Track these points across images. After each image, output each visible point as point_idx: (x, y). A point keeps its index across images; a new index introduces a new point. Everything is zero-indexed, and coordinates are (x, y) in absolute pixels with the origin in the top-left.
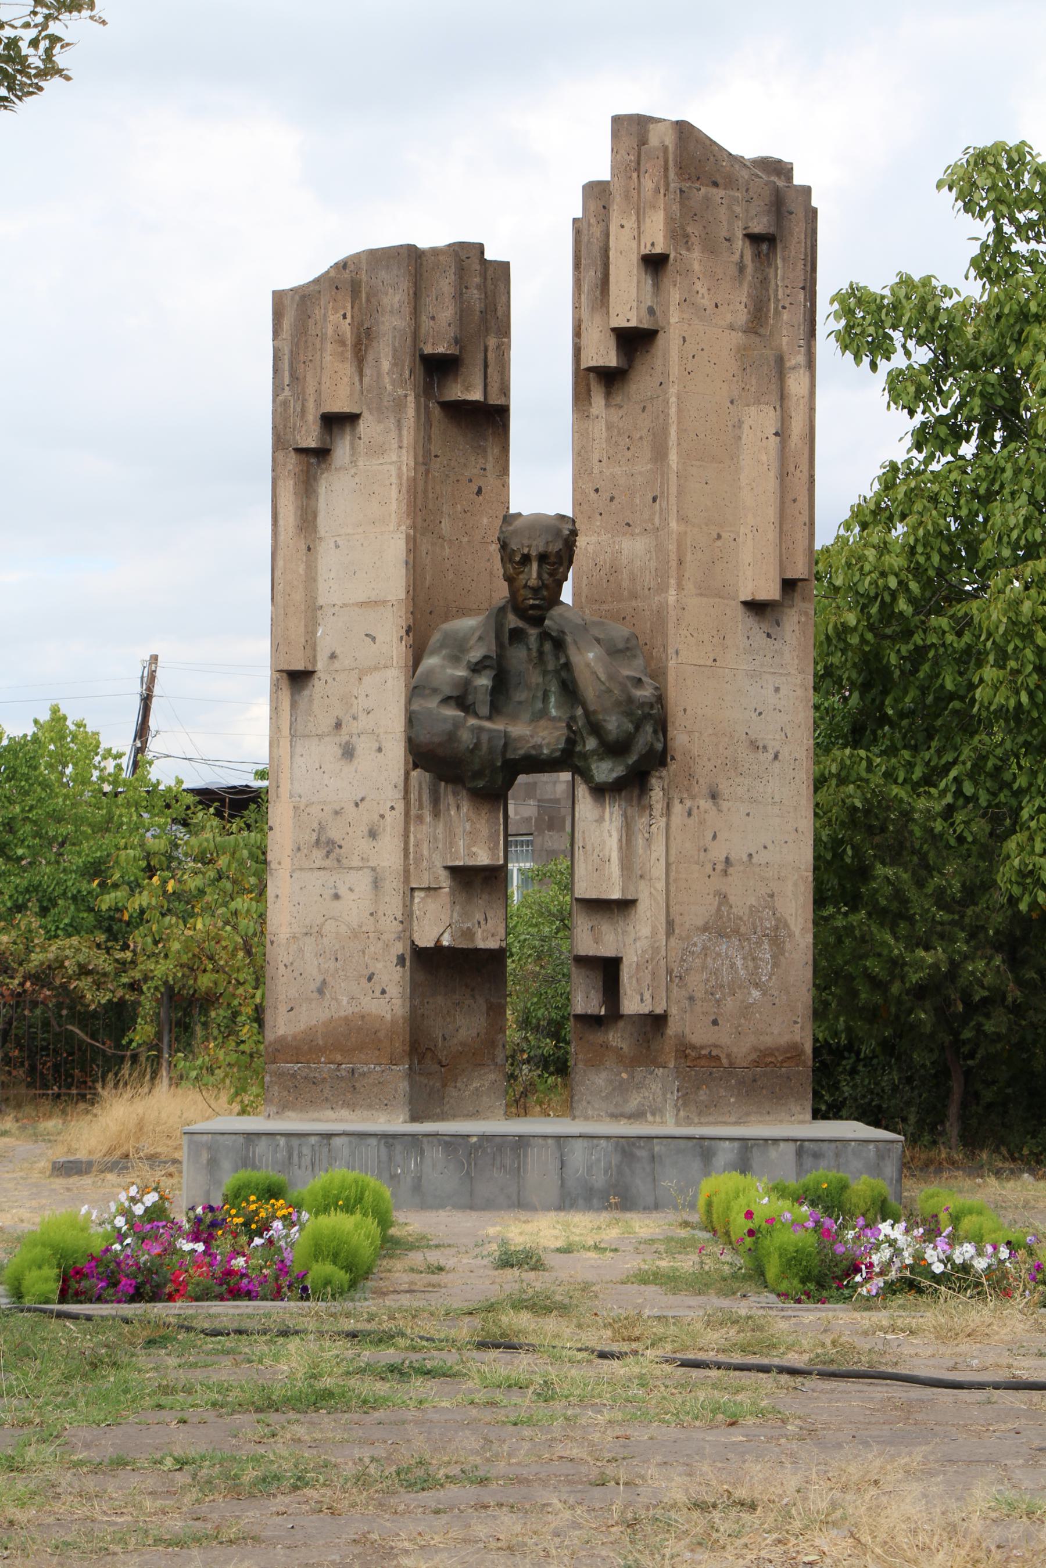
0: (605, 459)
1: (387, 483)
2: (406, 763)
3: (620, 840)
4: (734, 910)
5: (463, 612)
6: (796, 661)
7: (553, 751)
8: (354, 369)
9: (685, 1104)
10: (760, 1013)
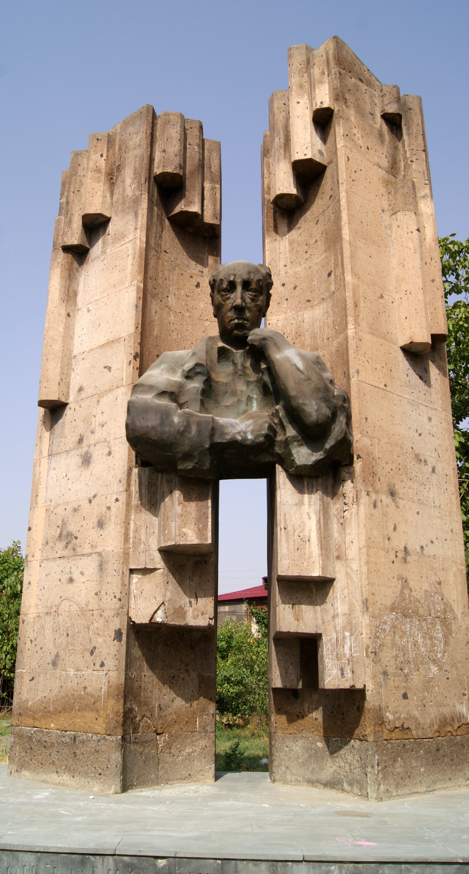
0: (289, 264)
1: (126, 256)
2: (130, 461)
3: (319, 522)
4: (414, 593)
7: (257, 436)
8: (106, 188)
9: (385, 778)
10: (439, 686)
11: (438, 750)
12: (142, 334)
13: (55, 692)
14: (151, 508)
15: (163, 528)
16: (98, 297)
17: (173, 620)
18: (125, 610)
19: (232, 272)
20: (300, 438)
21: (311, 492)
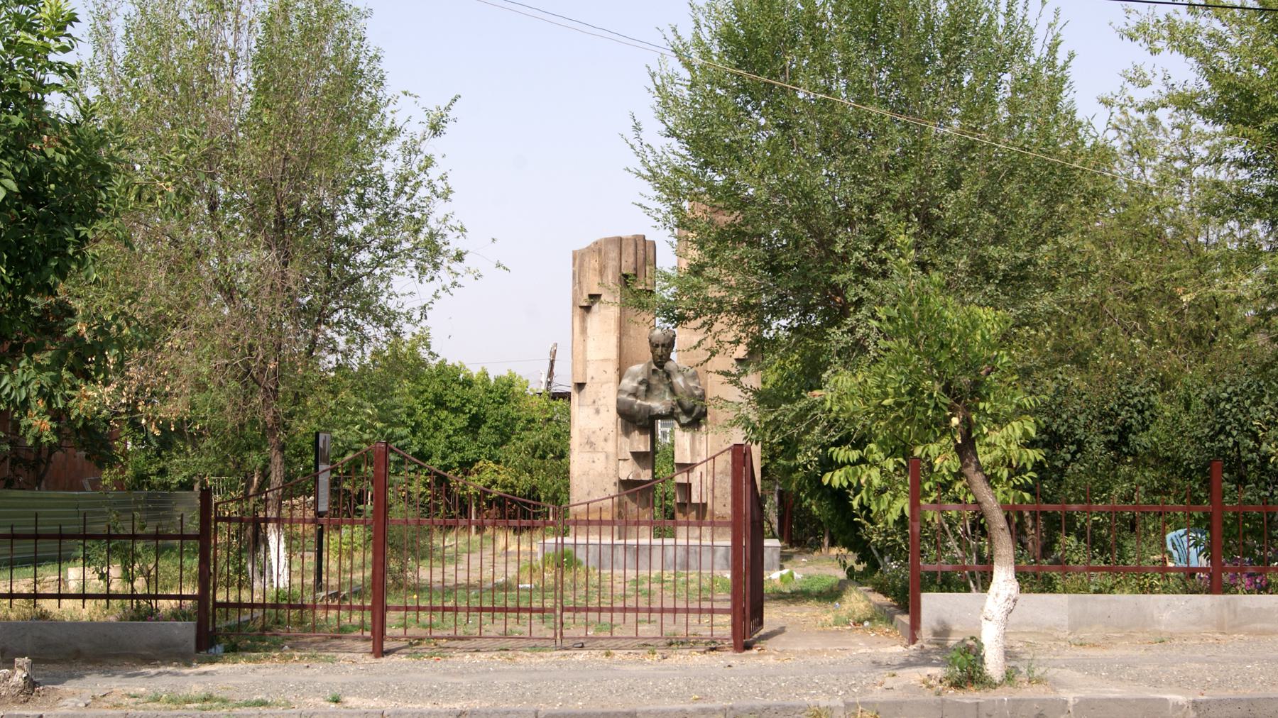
5: (638, 362)
15: (631, 444)
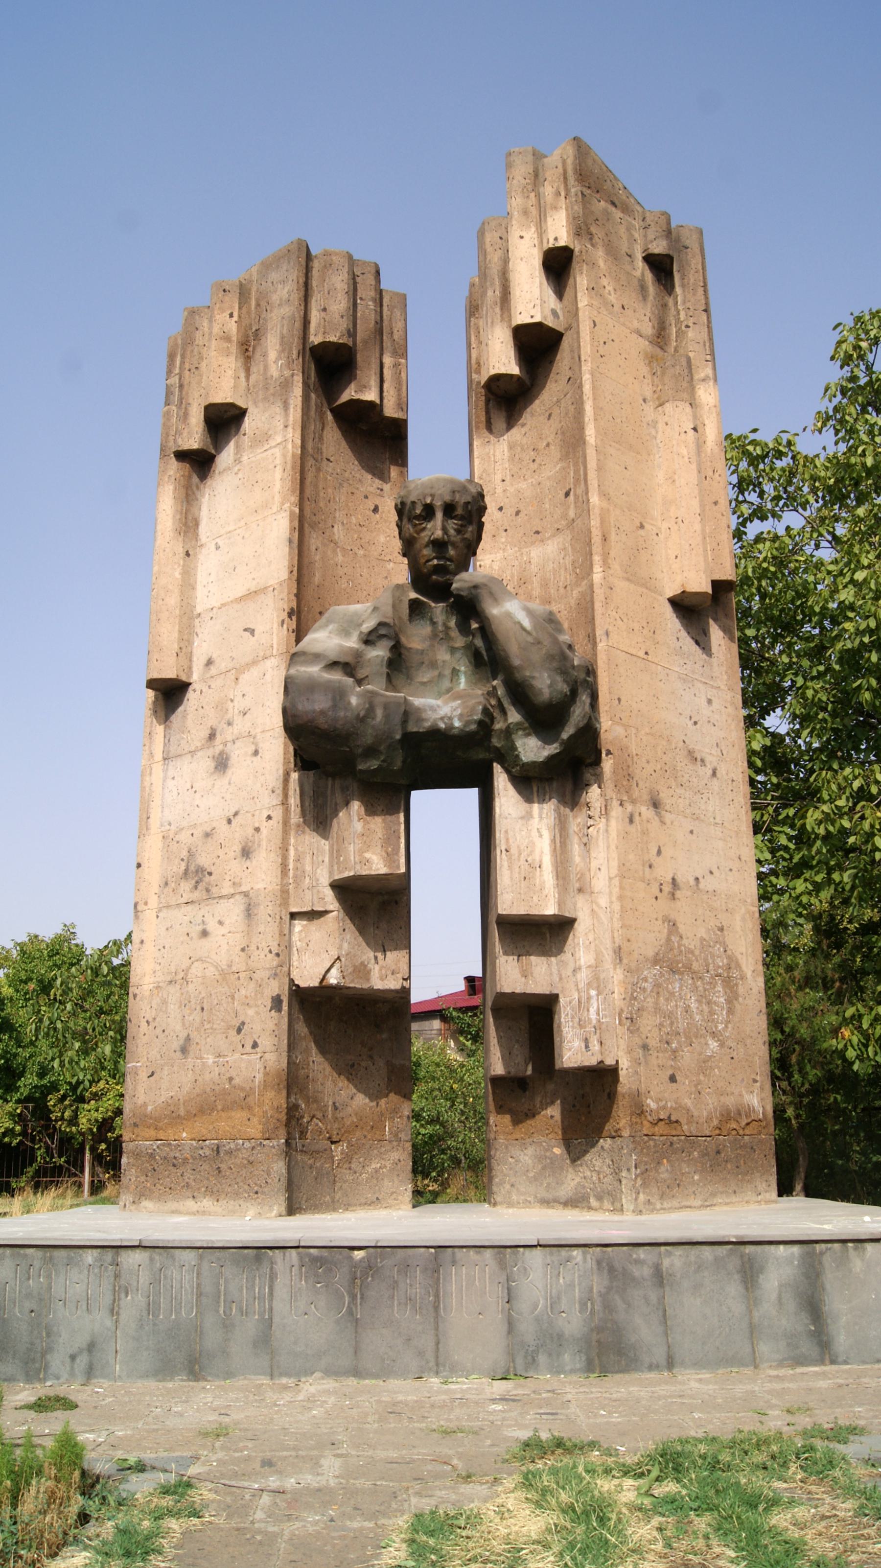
0: (508, 478)
1: (271, 466)
2: (286, 762)
3: (553, 841)
6: (725, 677)
7: (467, 723)
8: (239, 364)
9: (645, 1185)
11: (718, 1152)
12: (299, 581)
13: (186, 1089)
14: (318, 827)
15: (337, 854)
16: (231, 528)
17: (353, 981)
18: (285, 969)
19: (428, 491)
20: (527, 725)
21: (542, 801)
